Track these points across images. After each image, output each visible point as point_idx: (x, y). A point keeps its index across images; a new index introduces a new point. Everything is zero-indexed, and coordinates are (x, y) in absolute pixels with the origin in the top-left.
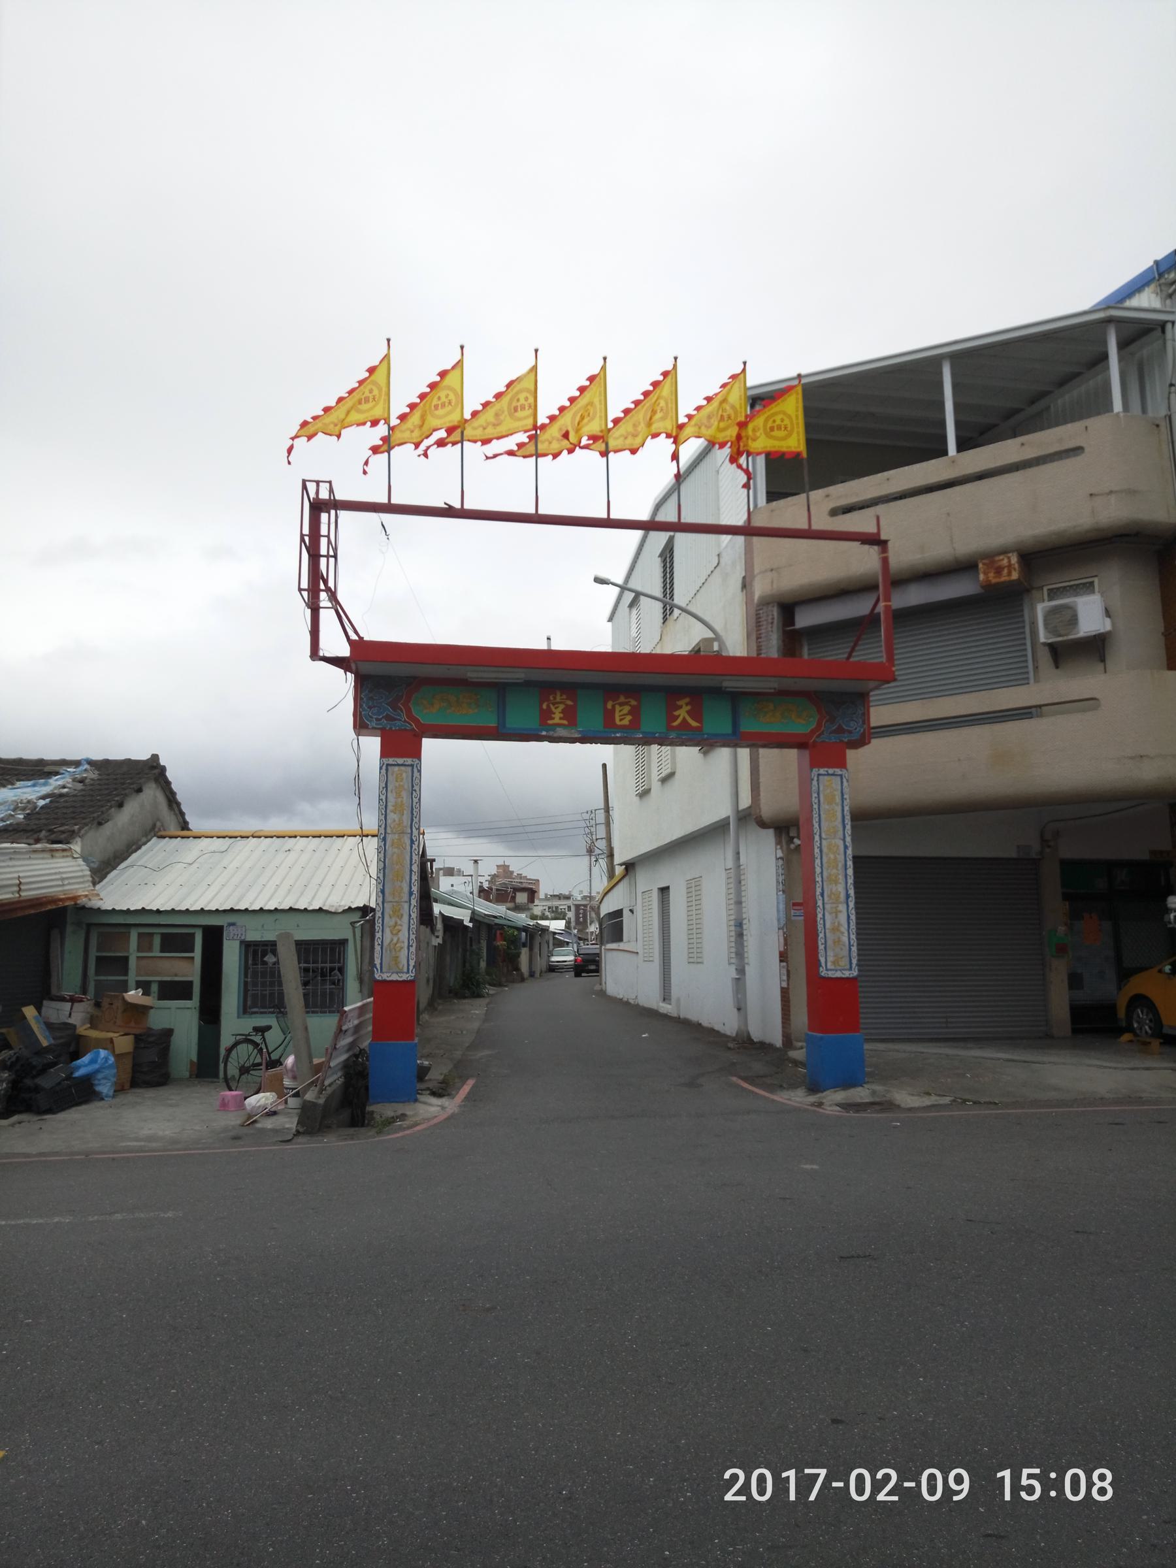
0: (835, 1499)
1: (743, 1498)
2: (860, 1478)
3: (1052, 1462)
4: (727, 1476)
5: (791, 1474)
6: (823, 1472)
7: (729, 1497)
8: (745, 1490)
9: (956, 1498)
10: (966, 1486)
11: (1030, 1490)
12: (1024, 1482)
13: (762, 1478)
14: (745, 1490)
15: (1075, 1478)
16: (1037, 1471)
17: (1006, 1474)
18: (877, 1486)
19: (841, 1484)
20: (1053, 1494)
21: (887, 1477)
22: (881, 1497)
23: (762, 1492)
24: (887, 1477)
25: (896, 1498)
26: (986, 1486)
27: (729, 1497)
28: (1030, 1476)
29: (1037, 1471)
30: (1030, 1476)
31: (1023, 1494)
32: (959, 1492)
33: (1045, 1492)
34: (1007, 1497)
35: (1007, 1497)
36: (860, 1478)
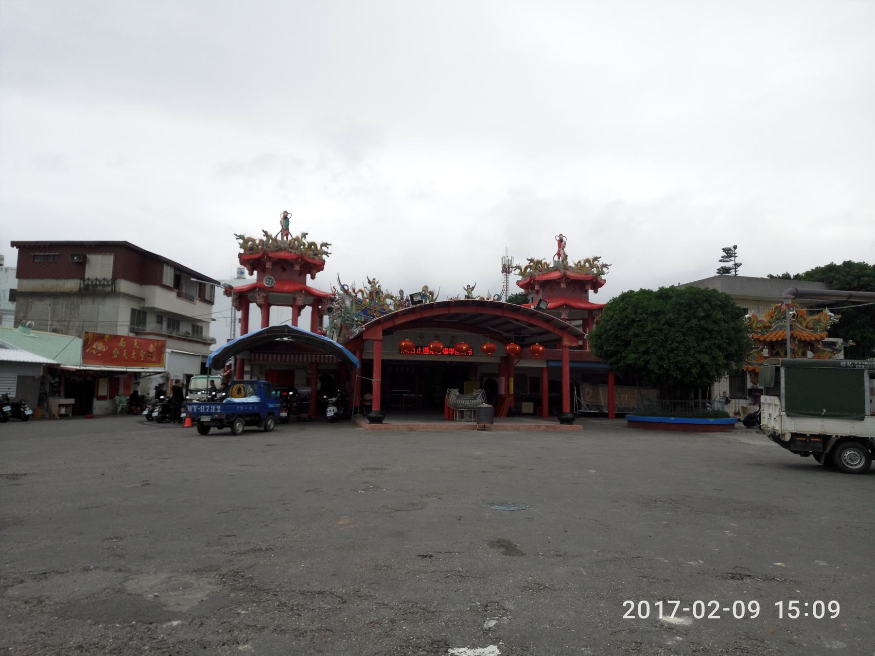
0: (727, 617)
1: (634, 617)
2: (699, 606)
3: (806, 598)
4: (624, 604)
5: (660, 603)
6: (678, 603)
7: (625, 616)
8: (635, 612)
9: (832, 617)
10: (758, 610)
11: (794, 612)
12: (790, 608)
13: (644, 606)
14: (635, 612)
15: (819, 606)
16: (797, 602)
17: (780, 604)
18: (708, 610)
19: (728, 609)
20: (806, 615)
21: (714, 605)
22: (710, 616)
23: (644, 613)
24: (714, 605)
25: (719, 617)
26: (769, 611)
27: (625, 616)
28: (793, 605)
29: (797, 602)
30: (793, 605)
31: (790, 615)
32: (834, 614)
33: (802, 613)
34: (781, 617)
35: (781, 617)
36: (699, 606)
